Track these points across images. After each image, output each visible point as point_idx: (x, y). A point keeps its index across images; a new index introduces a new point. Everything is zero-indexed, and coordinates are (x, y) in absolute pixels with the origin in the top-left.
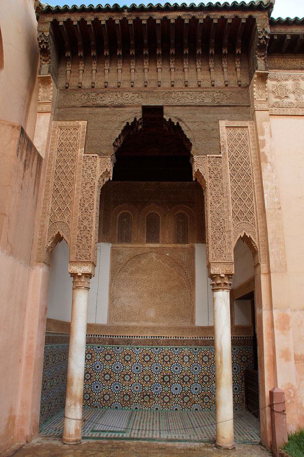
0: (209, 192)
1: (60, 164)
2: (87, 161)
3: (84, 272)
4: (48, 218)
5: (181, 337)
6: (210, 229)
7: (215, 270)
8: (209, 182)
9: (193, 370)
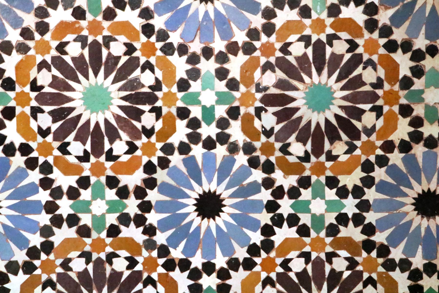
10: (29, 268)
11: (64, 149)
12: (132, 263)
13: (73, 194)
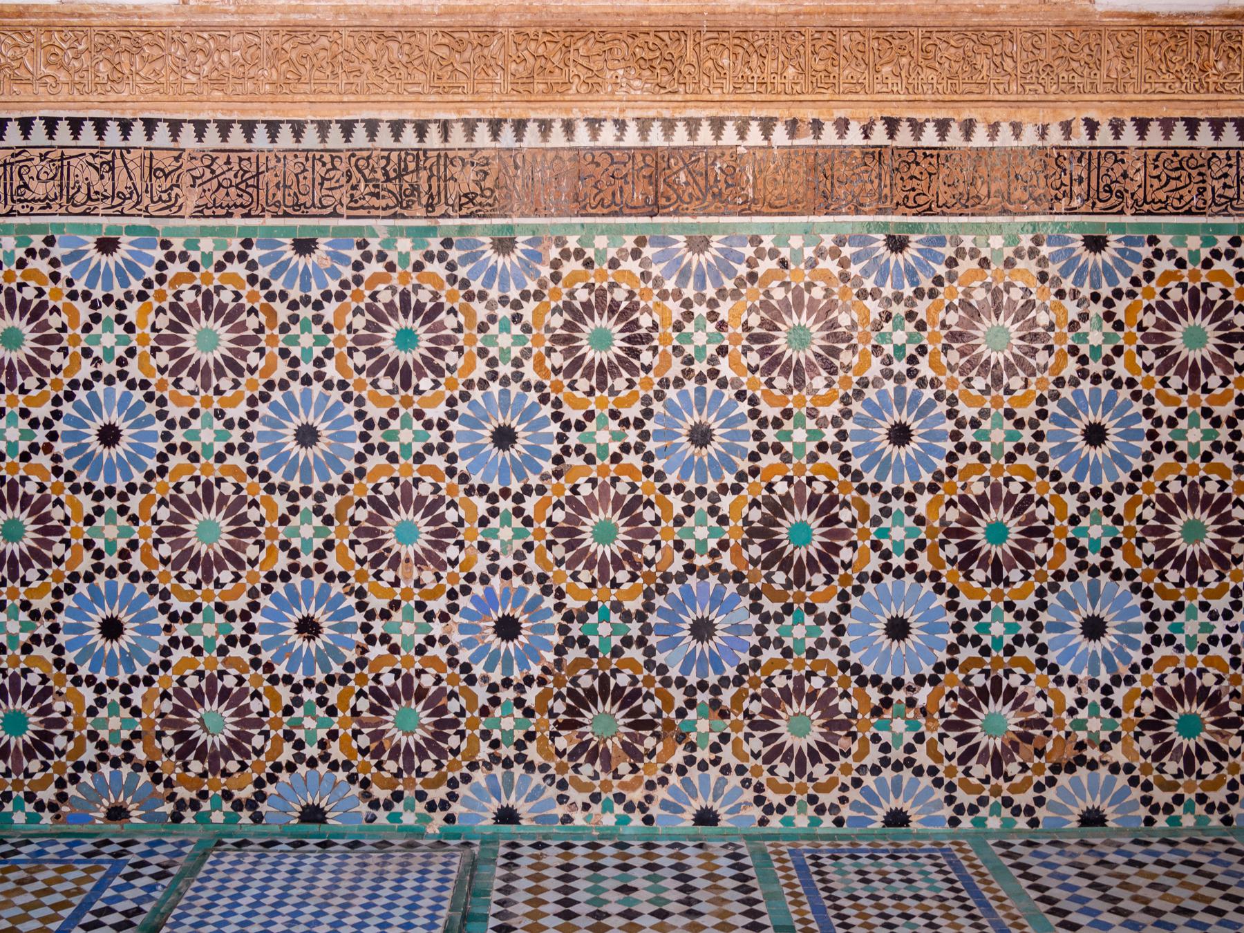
5: (943, 127)
9: (1066, 448)
10: (1132, 489)
11: (1164, 383)
12: (1223, 485)
13: (1172, 423)
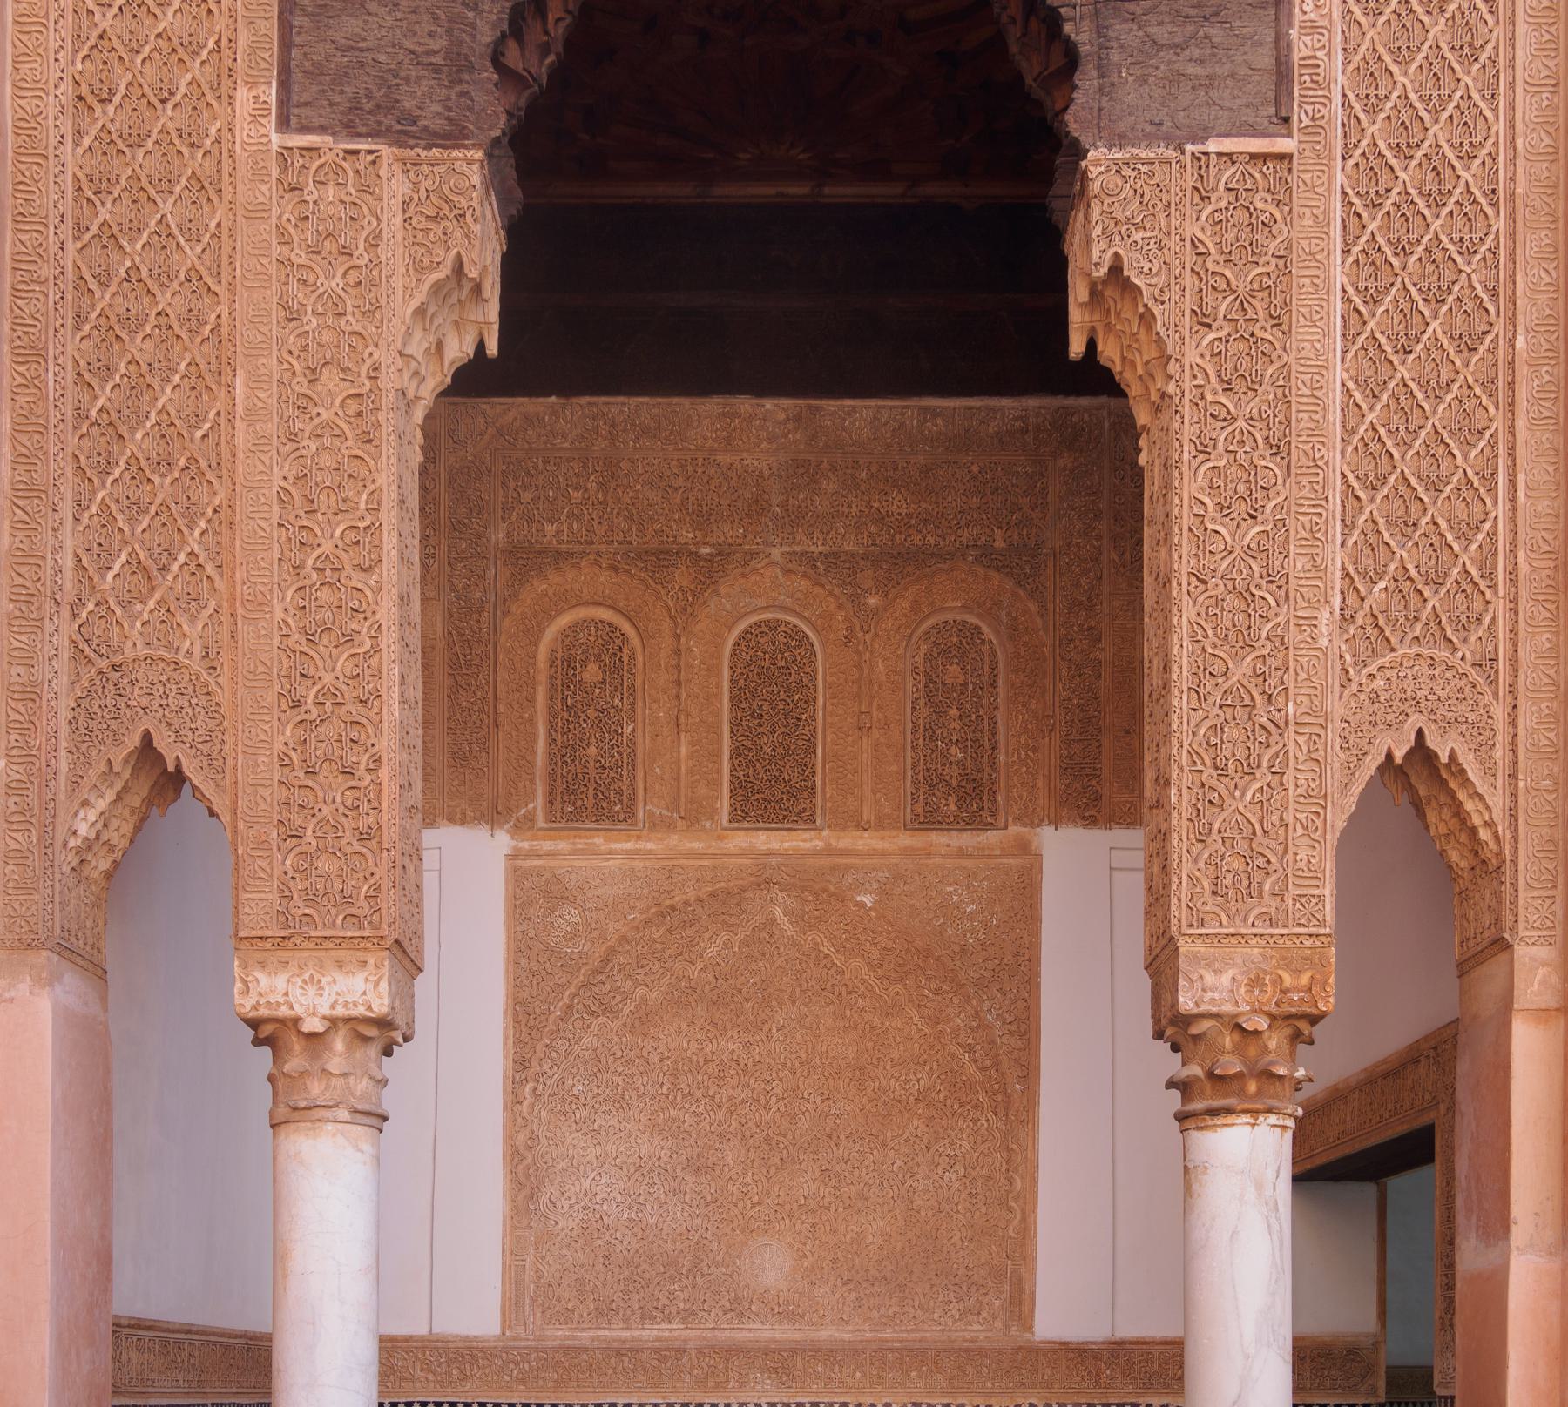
0: (1189, 431)
1: (103, 213)
2: (311, 193)
3: (340, 1011)
4: (61, 632)
6: (1181, 703)
7: (1213, 986)
8: (1191, 357)
